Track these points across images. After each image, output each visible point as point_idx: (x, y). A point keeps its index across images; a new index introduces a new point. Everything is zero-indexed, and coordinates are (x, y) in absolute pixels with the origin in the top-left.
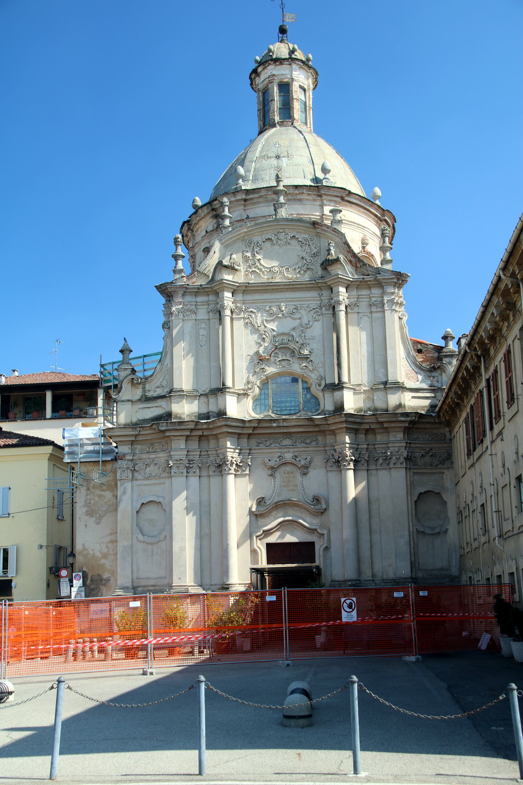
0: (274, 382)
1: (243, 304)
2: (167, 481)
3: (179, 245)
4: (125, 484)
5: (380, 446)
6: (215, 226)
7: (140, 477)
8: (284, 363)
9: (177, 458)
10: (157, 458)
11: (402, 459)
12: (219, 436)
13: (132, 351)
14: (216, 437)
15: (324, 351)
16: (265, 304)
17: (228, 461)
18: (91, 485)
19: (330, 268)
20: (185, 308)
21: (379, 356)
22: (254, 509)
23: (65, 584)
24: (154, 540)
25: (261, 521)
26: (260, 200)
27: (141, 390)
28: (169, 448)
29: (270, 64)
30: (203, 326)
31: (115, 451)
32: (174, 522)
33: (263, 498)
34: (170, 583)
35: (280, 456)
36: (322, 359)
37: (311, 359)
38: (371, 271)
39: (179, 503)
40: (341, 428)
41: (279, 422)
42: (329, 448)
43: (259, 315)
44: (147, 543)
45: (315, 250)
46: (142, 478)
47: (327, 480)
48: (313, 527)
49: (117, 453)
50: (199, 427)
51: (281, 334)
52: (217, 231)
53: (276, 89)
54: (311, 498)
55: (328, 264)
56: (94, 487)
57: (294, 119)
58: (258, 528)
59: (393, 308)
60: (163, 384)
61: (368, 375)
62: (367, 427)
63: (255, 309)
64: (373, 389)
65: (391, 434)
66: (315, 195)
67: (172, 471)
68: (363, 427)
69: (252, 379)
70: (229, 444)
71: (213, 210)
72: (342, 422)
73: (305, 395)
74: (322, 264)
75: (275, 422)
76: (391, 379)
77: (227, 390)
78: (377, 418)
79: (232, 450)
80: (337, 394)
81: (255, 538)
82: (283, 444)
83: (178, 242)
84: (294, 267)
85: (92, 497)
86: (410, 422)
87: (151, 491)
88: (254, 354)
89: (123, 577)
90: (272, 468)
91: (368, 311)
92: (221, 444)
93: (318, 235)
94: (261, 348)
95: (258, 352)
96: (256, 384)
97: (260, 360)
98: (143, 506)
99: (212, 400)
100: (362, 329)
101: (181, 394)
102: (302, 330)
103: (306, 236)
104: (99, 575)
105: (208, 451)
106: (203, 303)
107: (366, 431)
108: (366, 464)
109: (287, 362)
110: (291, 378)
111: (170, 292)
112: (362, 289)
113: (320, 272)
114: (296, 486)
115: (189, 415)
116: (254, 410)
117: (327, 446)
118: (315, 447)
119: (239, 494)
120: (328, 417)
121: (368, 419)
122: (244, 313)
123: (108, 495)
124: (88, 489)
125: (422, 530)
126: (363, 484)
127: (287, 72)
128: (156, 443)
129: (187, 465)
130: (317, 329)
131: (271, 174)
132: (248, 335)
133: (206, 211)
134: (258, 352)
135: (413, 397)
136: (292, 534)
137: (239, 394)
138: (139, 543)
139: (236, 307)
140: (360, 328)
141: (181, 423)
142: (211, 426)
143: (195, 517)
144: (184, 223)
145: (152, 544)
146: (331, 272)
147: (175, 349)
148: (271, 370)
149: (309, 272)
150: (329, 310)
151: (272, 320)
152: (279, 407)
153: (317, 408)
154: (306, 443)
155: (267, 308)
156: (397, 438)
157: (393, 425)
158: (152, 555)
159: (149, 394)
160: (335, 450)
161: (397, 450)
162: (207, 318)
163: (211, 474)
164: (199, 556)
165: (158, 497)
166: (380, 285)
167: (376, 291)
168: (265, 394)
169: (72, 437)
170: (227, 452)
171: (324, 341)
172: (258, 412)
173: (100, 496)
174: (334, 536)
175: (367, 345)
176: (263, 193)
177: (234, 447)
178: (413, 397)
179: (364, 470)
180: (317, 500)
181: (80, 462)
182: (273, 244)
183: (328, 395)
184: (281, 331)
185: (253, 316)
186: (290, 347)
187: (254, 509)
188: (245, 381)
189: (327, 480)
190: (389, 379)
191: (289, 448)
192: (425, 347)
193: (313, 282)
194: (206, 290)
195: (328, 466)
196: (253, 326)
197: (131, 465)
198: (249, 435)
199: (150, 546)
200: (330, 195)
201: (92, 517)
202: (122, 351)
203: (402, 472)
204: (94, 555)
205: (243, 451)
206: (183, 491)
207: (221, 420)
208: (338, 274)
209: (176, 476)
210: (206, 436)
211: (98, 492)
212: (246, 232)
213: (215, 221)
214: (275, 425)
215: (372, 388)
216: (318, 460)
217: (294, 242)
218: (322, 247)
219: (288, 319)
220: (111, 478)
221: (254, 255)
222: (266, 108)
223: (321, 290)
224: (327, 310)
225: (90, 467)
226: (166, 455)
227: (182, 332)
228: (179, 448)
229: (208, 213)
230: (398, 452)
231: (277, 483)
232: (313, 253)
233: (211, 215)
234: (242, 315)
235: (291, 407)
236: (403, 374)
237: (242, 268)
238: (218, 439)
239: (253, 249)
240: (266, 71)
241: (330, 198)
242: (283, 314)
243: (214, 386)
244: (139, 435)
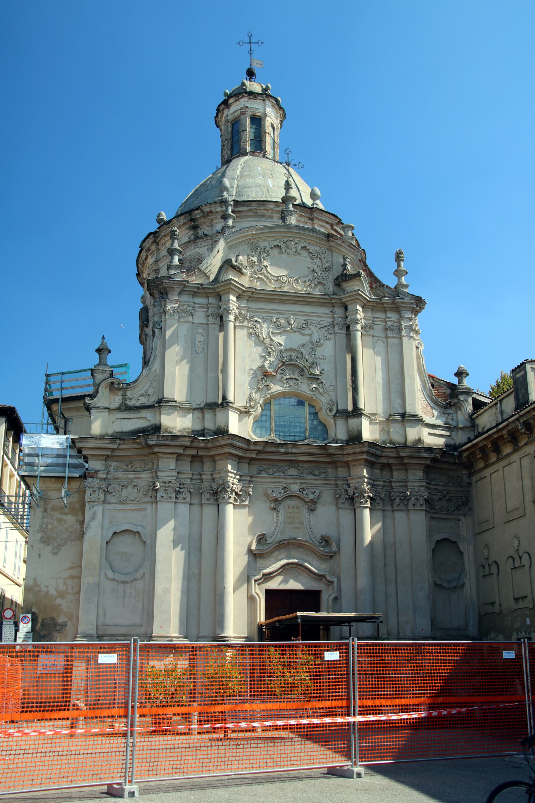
0: (277, 402)
1: (248, 311)
2: (149, 507)
3: (176, 238)
4: (95, 508)
5: (397, 484)
6: (192, 238)
7: (113, 500)
8: (292, 382)
9: (167, 479)
10: (137, 478)
11: (422, 501)
12: (217, 458)
13: (110, 352)
14: (213, 459)
15: (336, 373)
16: (271, 315)
17: (229, 488)
18: (49, 506)
19: (344, 285)
20: (182, 308)
21: (396, 384)
22: (253, 548)
23: (8, 628)
24: (127, 578)
25: (261, 562)
26: (250, 214)
27: (120, 397)
28: (155, 467)
29: (244, 96)
30: (200, 331)
31: (85, 466)
32: (158, 557)
33: (264, 535)
34: (149, 632)
35: (285, 488)
36: (334, 383)
37: (322, 380)
38: (388, 293)
39: (165, 534)
40: (359, 460)
41: (287, 448)
42: (342, 482)
43: (265, 325)
44: (118, 582)
45: (327, 265)
46: (116, 501)
47: (338, 519)
48: (321, 573)
49: (87, 469)
50: (195, 445)
51: (289, 349)
52: (195, 242)
53: (248, 121)
54: (319, 539)
55: (343, 279)
56: (54, 509)
57: (266, 152)
58: (256, 570)
59: (411, 335)
60: (149, 392)
61: (384, 404)
62: (385, 461)
63: (261, 319)
64: (389, 419)
65: (410, 472)
66: (306, 217)
67: (159, 494)
68: (380, 461)
69: (256, 396)
70: (229, 467)
71: (192, 220)
72: (361, 453)
73: (312, 420)
74: (337, 279)
75: (282, 447)
76: (409, 410)
77: (230, 405)
78: (398, 452)
79: (233, 475)
80: (353, 422)
81: (253, 582)
82: (288, 474)
83: (176, 235)
84: (304, 279)
85: (49, 521)
86: (434, 460)
87: (128, 519)
88: (258, 369)
89: (87, 622)
90: (276, 500)
91: (382, 334)
92: (218, 467)
93: (331, 249)
94: (267, 362)
95: (262, 367)
96: (259, 403)
97: (264, 375)
98: (115, 536)
99: (208, 416)
100: (377, 353)
101: (173, 406)
102: (312, 348)
103: (318, 249)
104: (53, 619)
105: (201, 475)
106: (202, 305)
107: (382, 466)
108: (381, 504)
109: (294, 381)
110: (296, 401)
111: (165, 288)
112: (378, 311)
113: (331, 287)
114: (302, 523)
115: (180, 431)
116: (254, 432)
117: (340, 480)
118: (324, 480)
119: (238, 527)
120: (346, 446)
121: (388, 452)
122: (248, 322)
123: (71, 520)
124: (45, 511)
125: (439, 583)
126: (379, 526)
127: (260, 107)
128: (138, 460)
129: (178, 489)
130: (328, 349)
131: (257, 192)
132: (251, 346)
133: (182, 220)
134: (263, 366)
135: (430, 434)
136: (295, 580)
137: (241, 412)
138: (108, 581)
139: (240, 314)
140: (375, 352)
141: (175, 437)
142: (210, 445)
143: (183, 552)
144: (150, 234)
145: (123, 582)
146: (347, 289)
147: (167, 353)
148: (276, 388)
149: (319, 287)
150: (342, 329)
151: (279, 333)
152: (282, 432)
153: (325, 436)
154: (314, 475)
155: (274, 319)
156: (417, 475)
157: (414, 461)
158: (124, 597)
160: (349, 485)
161: (417, 489)
162: (206, 322)
163: (203, 502)
164: (186, 600)
165: (136, 525)
166: (397, 309)
167: (392, 316)
168: (266, 416)
169: (32, 445)
170: (228, 476)
171: (335, 363)
172: (258, 435)
173: (60, 520)
174: (346, 585)
175: (382, 372)
176: (254, 206)
177: (235, 472)
178: (430, 434)
179: (380, 510)
180: (326, 541)
181: (41, 477)
182: (281, 252)
183: (340, 423)
184: (289, 347)
185: (258, 326)
186: (300, 365)
187: (253, 548)
188: (247, 397)
189: (338, 519)
190: (407, 411)
191: (296, 479)
192: (437, 382)
193: (327, 297)
194: (207, 291)
195: (340, 502)
196: (258, 337)
197: (104, 485)
198: (251, 459)
199: (122, 586)
200: (321, 220)
201: (48, 545)
202: (99, 351)
203: (423, 515)
204: (47, 593)
205: (243, 478)
206: (170, 520)
207: (226, 437)
208: (359, 290)
209: (163, 501)
210: (201, 457)
211: (57, 515)
212: (253, 234)
213: (192, 232)
214: (282, 450)
215: (387, 419)
216: (327, 496)
217: (304, 253)
218: (334, 262)
219: (297, 334)
220: (75, 500)
221: (260, 261)
222: (235, 138)
223: (334, 307)
224: (340, 329)
225: (51, 484)
226: (150, 475)
227: (175, 335)
228: (169, 468)
229: (184, 224)
230: (417, 492)
231: (280, 518)
232: (324, 267)
233: (187, 226)
234: (246, 324)
235: (295, 432)
236: (420, 407)
237: (248, 272)
238: (215, 462)
239: (260, 255)
240: (238, 103)
241: (321, 223)
242: (291, 328)
243: (211, 400)
244: (117, 449)
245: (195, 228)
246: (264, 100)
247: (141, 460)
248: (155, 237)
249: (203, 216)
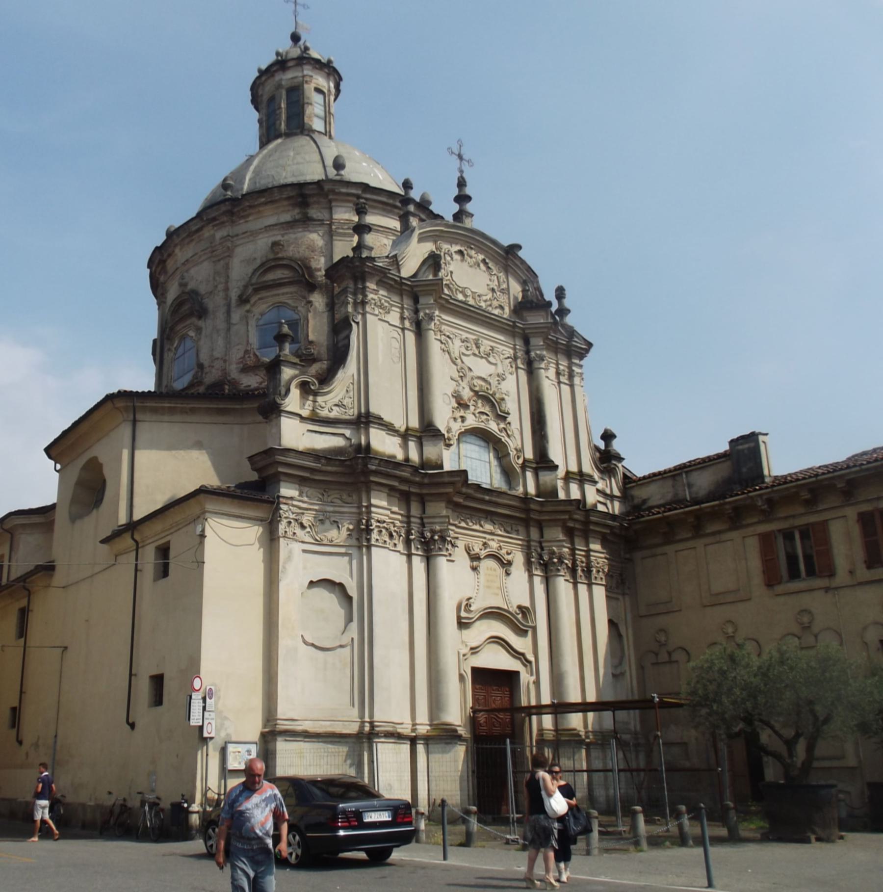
75: (488, 495)
159: (324, 413)
194: (404, 287)
213: (297, 211)
214: (487, 498)
229: (288, 198)
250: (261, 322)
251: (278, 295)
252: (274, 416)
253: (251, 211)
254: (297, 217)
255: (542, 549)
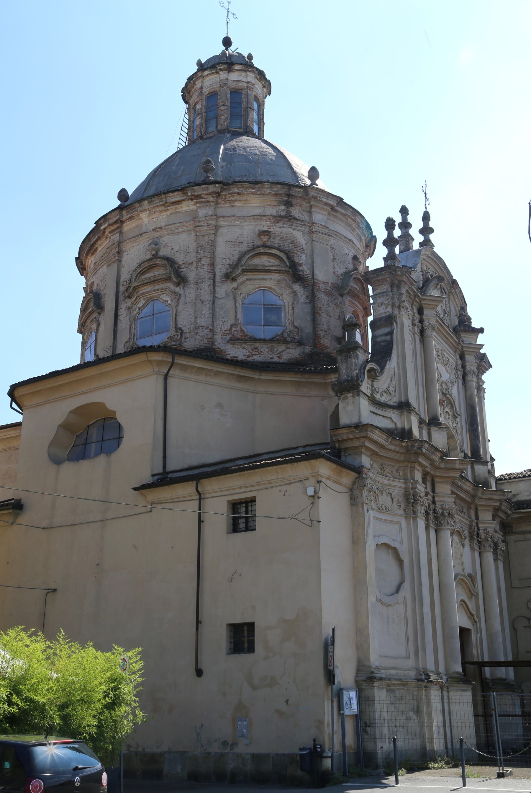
146: (464, 339)
213: (282, 207)
229: (276, 195)
240: (243, 74)
245: (288, 204)
246: (264, 87)
247: (392, 466)
248: (222, 188)
249: (303, 199)
250: (246, 301)
251: (266, 280)
252: (351, 395)
253: (237, 197)
254: (283, 214)
255: (479, 529)
